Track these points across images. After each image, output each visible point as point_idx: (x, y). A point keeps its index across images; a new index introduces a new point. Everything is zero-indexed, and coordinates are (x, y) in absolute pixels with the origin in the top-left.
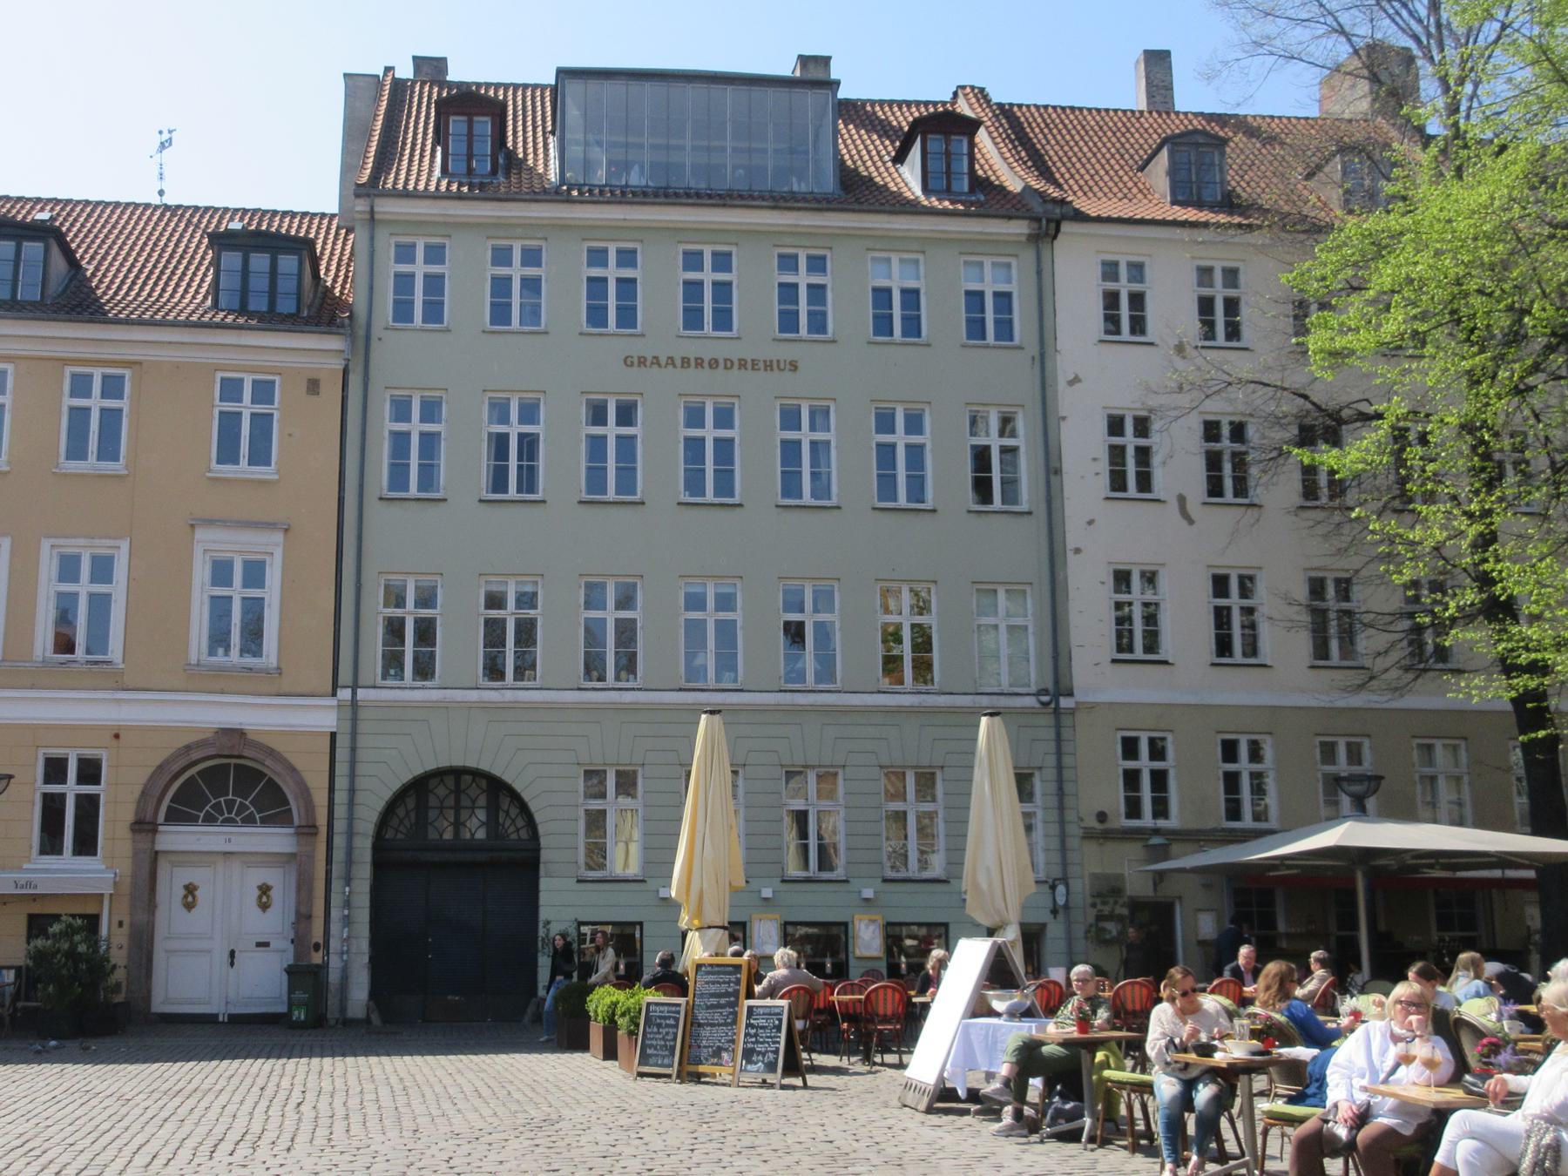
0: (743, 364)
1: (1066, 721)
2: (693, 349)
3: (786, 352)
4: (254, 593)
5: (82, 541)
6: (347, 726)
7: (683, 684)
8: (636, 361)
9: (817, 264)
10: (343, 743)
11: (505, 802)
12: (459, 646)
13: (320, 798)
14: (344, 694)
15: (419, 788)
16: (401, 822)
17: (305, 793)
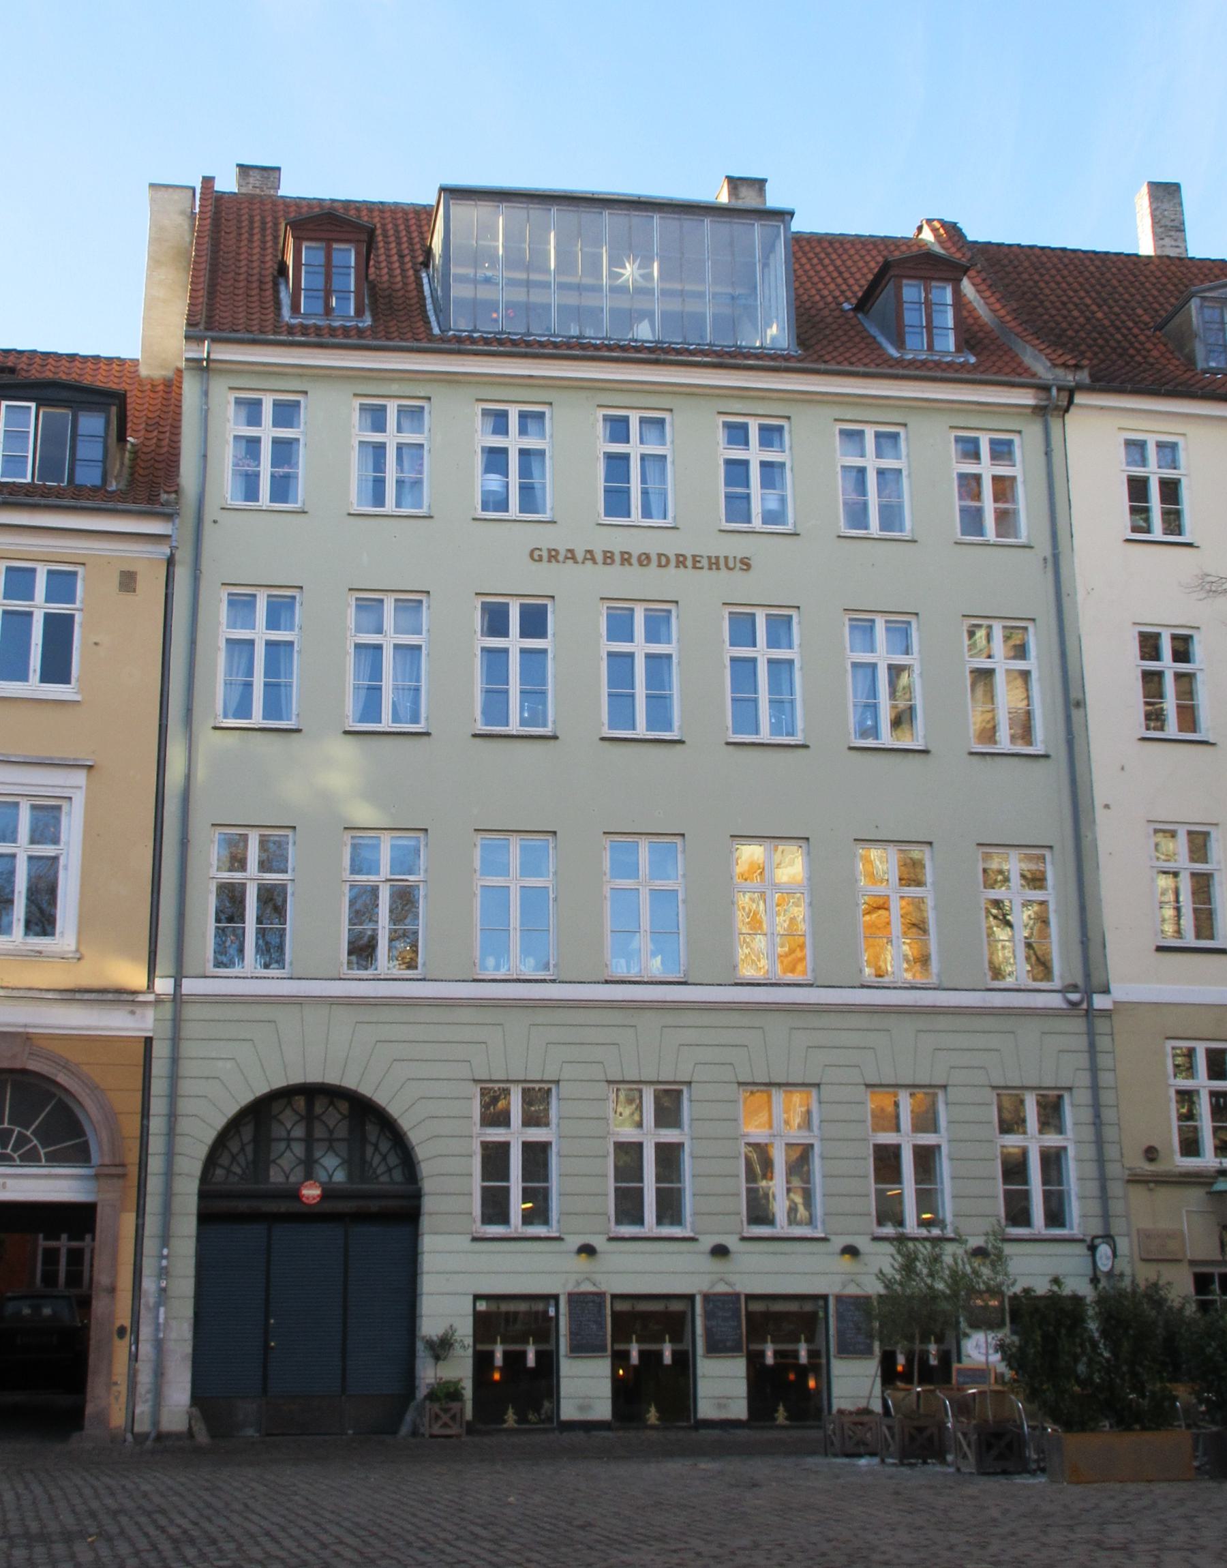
0: (681, 561)
1: (1101, 1025)
2: (618, 542)
3: (735, 547)
4: (47, 850)
8: (545, 554)
9: (770, 435)
10: (161, 1051)
12: (318, 924)
13: (131, 1126)
15: (259, 1114)
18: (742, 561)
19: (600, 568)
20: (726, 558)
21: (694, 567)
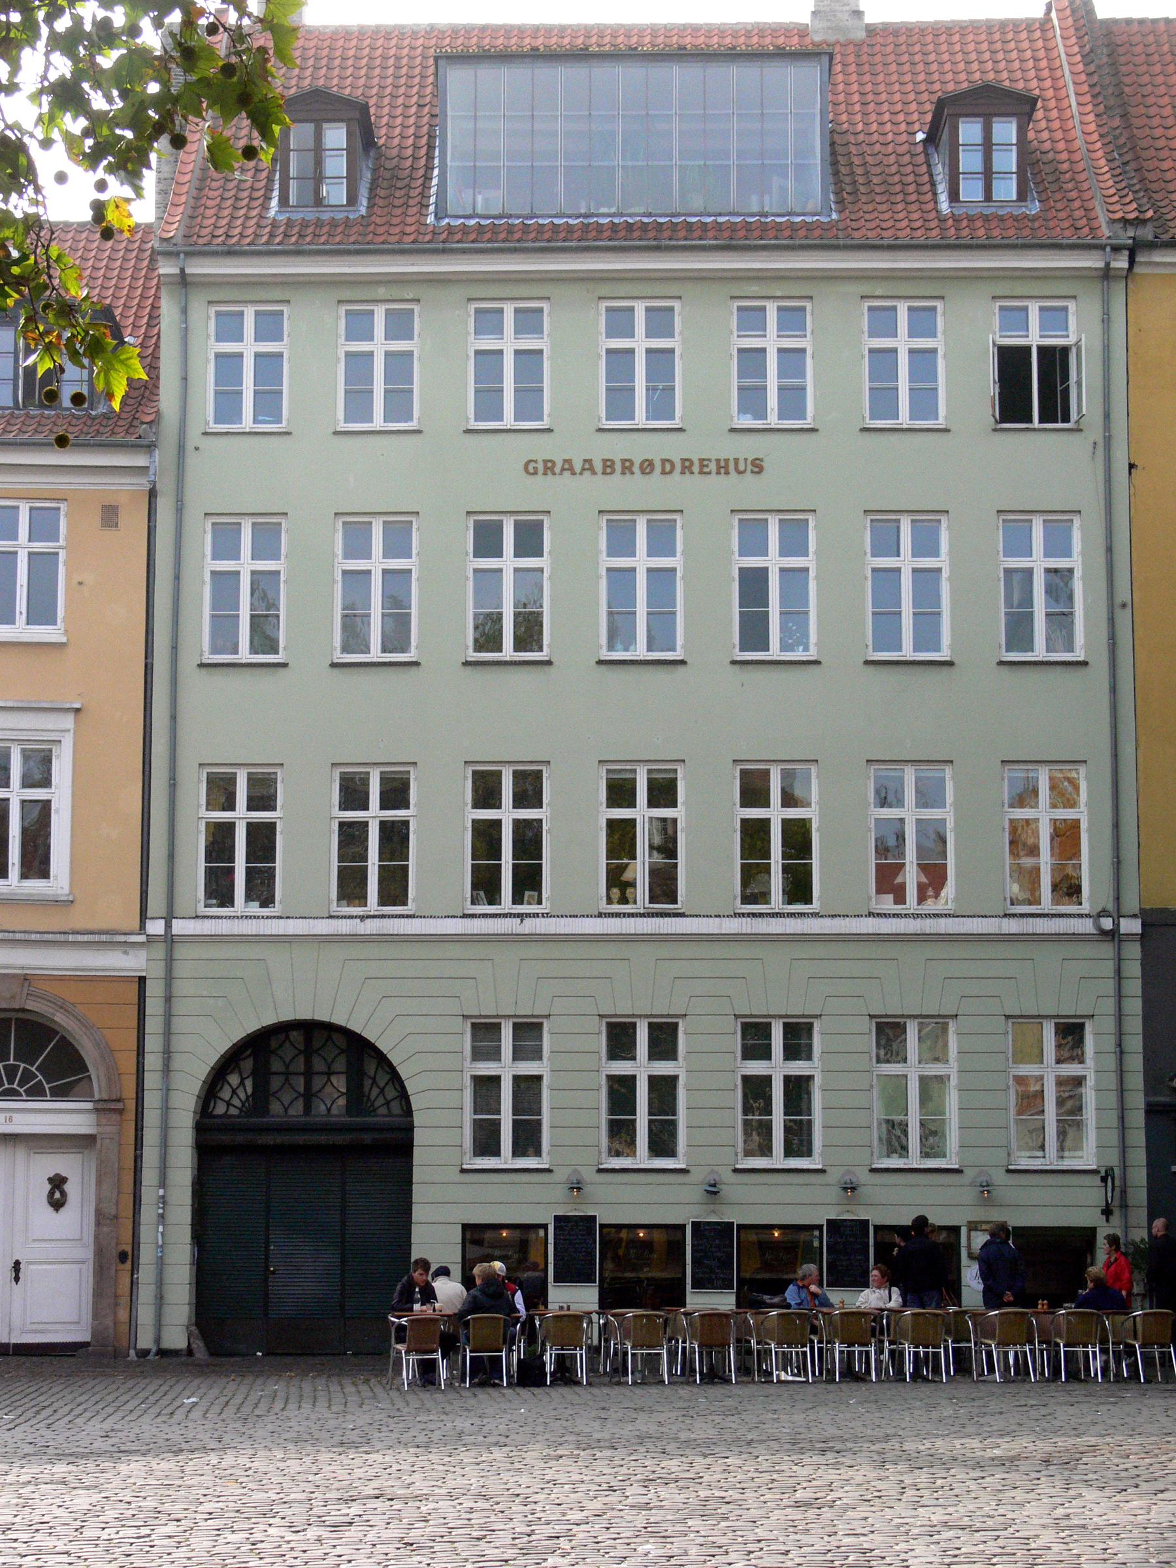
0: (687, 466)
3: (746, 448)
7: (604, 907)
10: (154, 991)
11: (371, 1067)
13: (128, 1063)
14: (156, 927)
16: (234, 1092)
17: (108, 1053)
18: (753, 463)
19: (599, 477)
20: (736, 460)
21: (701, 472)
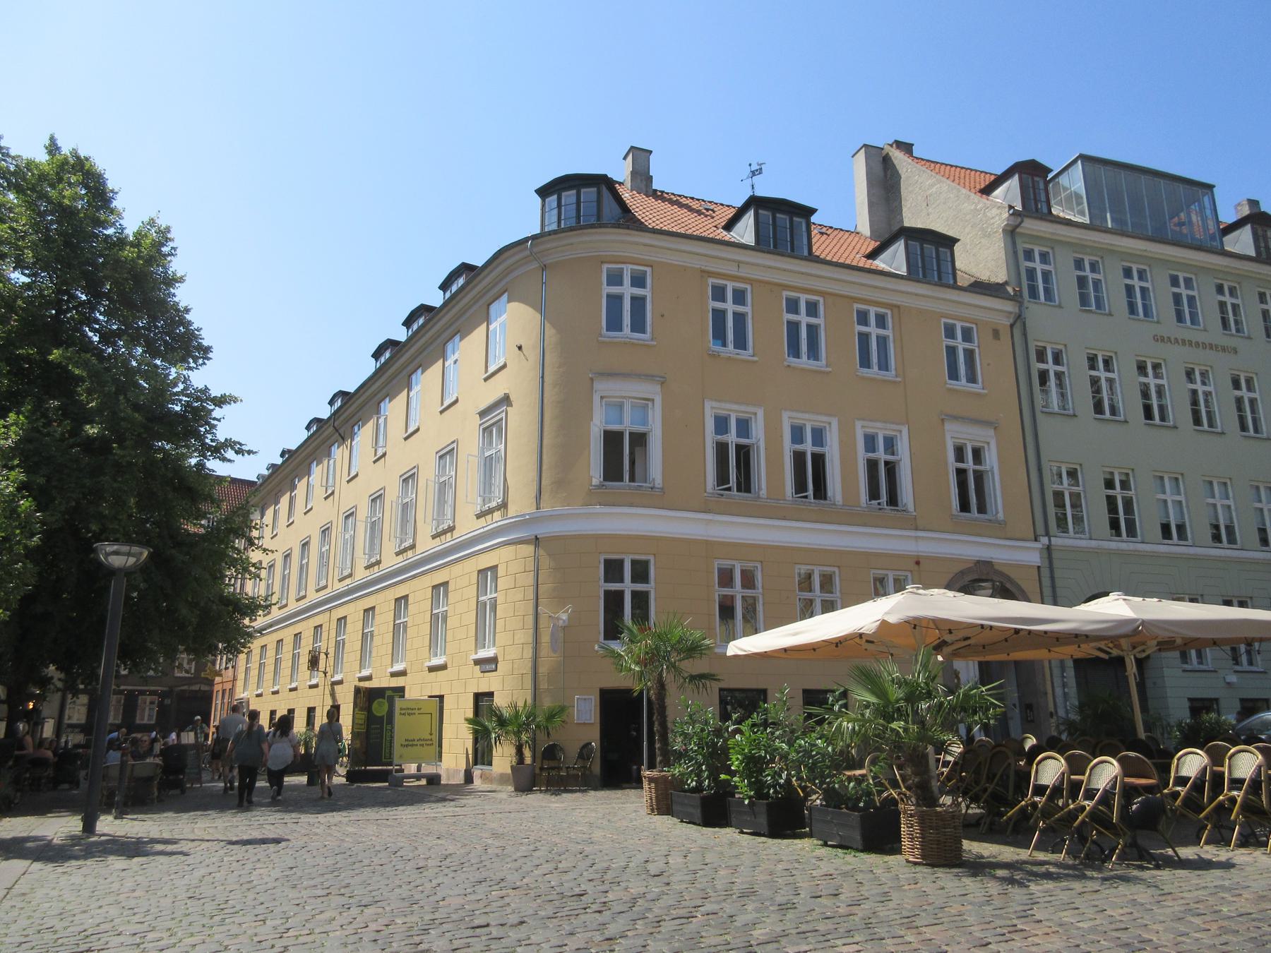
5: (879, 425)
6: (1046, 564)
